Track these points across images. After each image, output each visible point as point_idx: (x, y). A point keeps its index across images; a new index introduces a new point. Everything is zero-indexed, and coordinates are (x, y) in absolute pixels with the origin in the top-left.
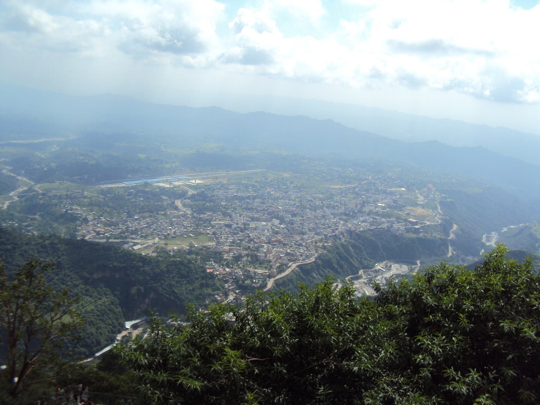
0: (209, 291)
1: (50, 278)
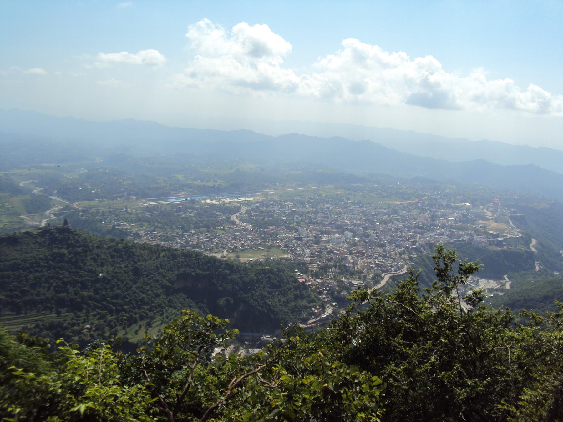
0: (305, 303)
1: (128, 286)
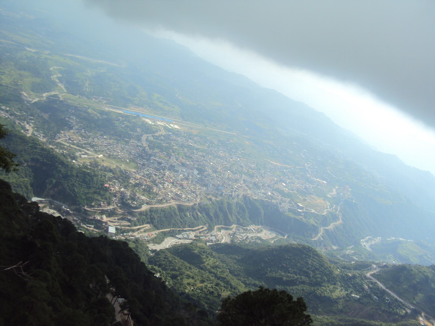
0: (99, 198)
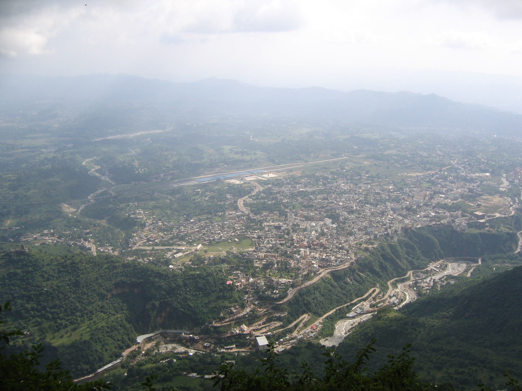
0: (226, 303)
